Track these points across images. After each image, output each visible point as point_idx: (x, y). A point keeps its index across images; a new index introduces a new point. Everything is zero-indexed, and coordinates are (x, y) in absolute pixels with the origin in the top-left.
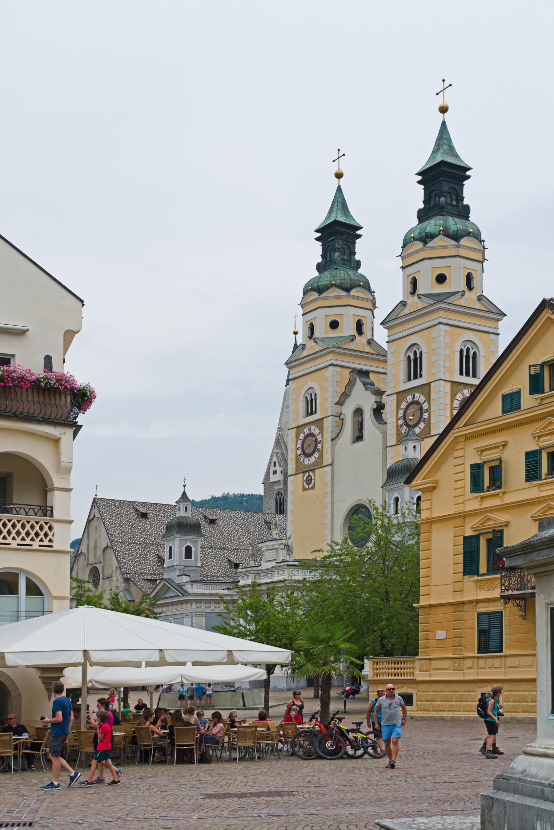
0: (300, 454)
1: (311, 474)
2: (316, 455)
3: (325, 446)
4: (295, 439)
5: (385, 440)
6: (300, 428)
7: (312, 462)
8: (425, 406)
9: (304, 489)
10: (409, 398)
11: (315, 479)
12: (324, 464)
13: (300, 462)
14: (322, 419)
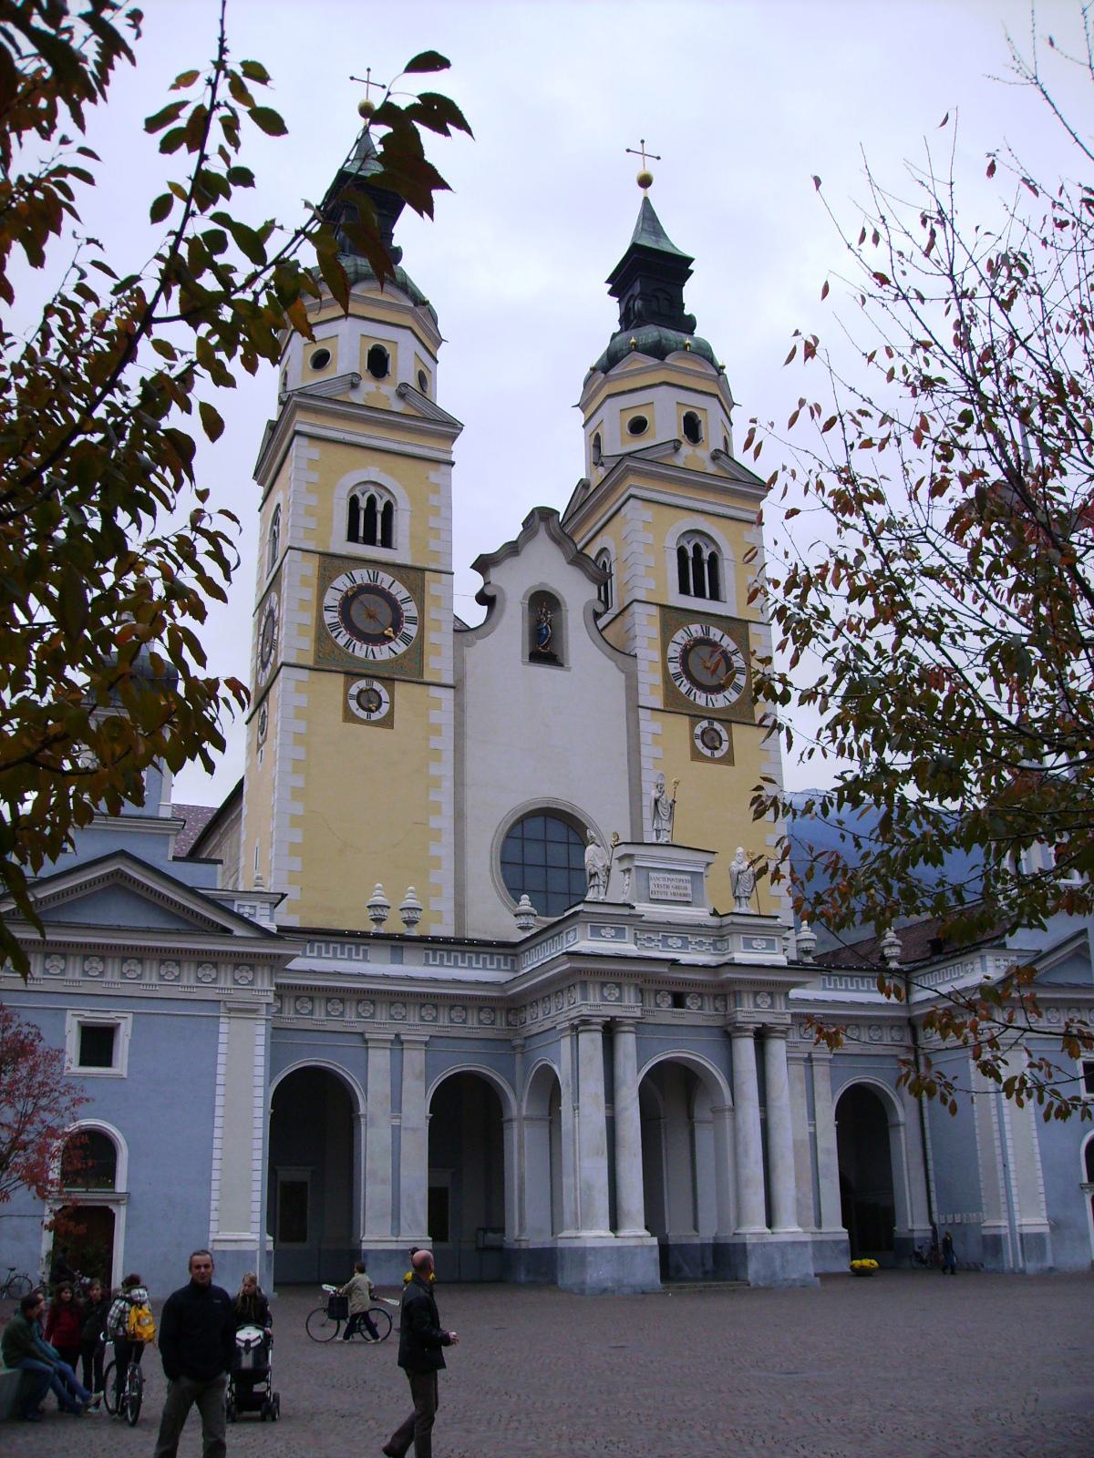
0: (334, 626)
1: (377, 686)
2: (400, 647)
3: (431, 637)
4: (315, 581)
5: (632, 689)
6: (337, 562)
7: (380, 657)
9: (349, 716)
10: (696, 630)
11: (392, 703)
12: (427, 678)
14: (423, 570)
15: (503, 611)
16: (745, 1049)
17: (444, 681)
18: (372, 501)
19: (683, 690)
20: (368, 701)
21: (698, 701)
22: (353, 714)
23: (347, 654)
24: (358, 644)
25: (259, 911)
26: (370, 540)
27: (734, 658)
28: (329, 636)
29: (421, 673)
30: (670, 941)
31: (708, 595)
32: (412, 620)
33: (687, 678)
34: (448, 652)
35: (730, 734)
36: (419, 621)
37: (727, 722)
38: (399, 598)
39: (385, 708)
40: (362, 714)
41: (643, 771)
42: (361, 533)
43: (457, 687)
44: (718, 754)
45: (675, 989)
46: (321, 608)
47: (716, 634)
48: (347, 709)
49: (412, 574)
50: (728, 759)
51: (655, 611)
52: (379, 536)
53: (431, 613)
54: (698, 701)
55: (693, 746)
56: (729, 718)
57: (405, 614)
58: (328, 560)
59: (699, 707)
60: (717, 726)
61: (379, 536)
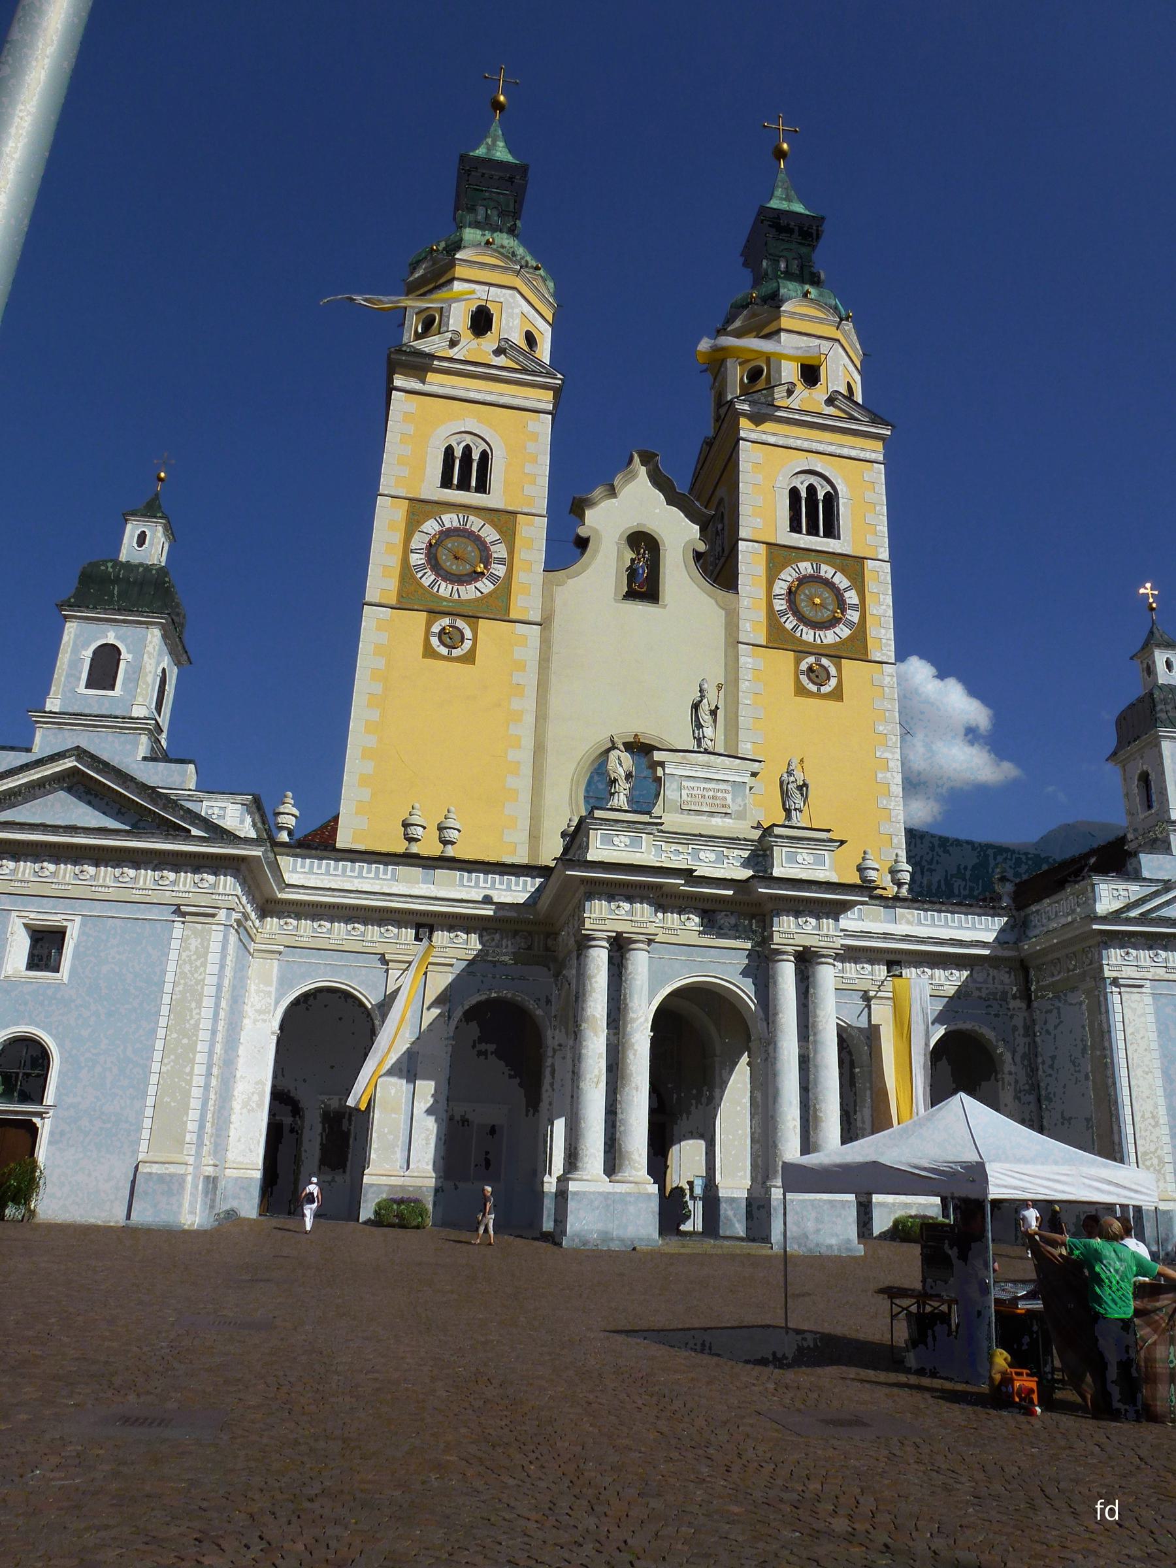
1: (460, 623)
2: (486, 586)
3: (519, 577)
7: (464, 597)
8: (852, 597)
9: (429, 652)
10: (806, 567)
12: (513, 616)
13: (422, 586)
15: (596, 551)
16: (787, 973)
17: (531, 619)
18: (467, 450)
19: (789, 626)
20: (451, 638)
21: (804, 637)
22: (434, 651)
23: (432, 594)
24: (444, 584)
25: (229, 812)
26: (464, 485)
27: (847, 595)
28: (414, 578)
29: (508, 610)
30: (702, 855)
31: (821, 534)
32: (501, 561)
33: (794, 614)
34: (537, 591)
35: (839, 670)
36: (509, 562)
37: (836, 658)
38: (488, 540)
39: (467, 645)
40: (444, 651)
41: (740, 706)
42: (455, 481)
43: (544, 624)
44: (825, 689)
45: (707, 906)
46: (407, 551)
47: (827, 571)
48: (427, 643)
49: (504, 517)
50: (837, 695)
51: (762, 548)
52: (473, 483)
53: (521, 555)
54: (804, 637)
55: (798, 681)
56: (837, 654)
57: (495, 555)
58: (418, 505)
59: (806, 643)
60: (825, 661)
61: (473, 483)
